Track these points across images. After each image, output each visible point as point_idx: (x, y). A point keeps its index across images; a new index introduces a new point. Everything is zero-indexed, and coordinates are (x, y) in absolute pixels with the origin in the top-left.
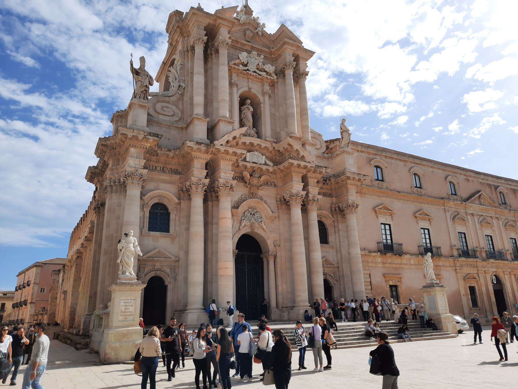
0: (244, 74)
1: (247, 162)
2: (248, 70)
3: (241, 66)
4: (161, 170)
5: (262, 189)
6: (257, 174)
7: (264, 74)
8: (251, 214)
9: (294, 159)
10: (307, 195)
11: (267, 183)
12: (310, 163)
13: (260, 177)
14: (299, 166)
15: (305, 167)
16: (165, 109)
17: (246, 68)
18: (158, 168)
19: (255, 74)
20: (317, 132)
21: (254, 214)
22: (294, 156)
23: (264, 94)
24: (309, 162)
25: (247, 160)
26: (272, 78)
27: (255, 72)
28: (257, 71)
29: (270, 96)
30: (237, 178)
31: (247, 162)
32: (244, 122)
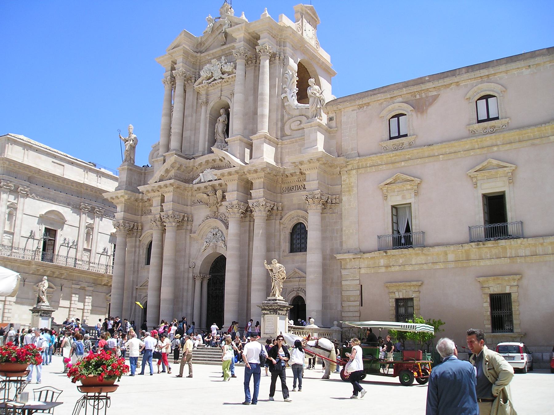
1: (203, 182)
17: (213, 79)
31: (203, 182)
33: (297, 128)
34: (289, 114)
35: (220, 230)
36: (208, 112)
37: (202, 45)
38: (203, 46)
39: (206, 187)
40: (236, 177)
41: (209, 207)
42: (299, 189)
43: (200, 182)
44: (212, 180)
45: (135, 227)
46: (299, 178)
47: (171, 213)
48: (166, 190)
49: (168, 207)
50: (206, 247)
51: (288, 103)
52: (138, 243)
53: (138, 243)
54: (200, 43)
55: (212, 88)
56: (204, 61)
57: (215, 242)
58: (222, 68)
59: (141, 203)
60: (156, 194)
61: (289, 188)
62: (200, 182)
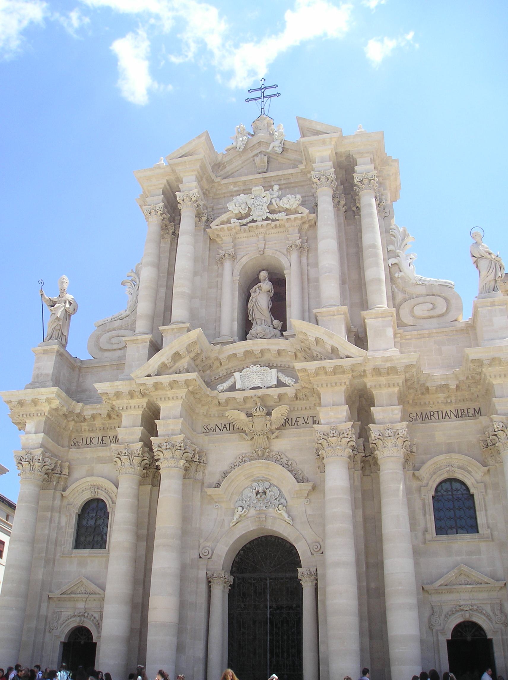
0: (245, 231)
1: (238, 390)
4: (99, 443)
5: (277, 437)
6: (258, 409)
8: (258, 493)
9: (321, 359)
11: (297, 421)
13: (269, 414)
16: (114, 340)
17: (250, 219)
18: (95, 441)
21: (265, 493)
22: (320, 353)
25: (238, 387)
27: (267, 219)
28: (270, 216)
30: (228, 426)
31: (238, 390)
33: (426, 314)
34: (404, 292)
35: (274, 485)
36: (237, 272)
37: (221, 168)
38: (221, 170)
39: (245, 399)
40: (346, 378)
41: (249, 438)
42: (447, 417)
43: (233, 388)
44: (260, 388)
45: (58, 469)
46: (448, 397)
47: (180, 441)
48: (169, 393)
49: (171, 427)
50: (240, 516)
51: (401, 274)
52: (58, 502)
53: (58, 502)
54: (219, 163)
55: (245, 235)
56: (224, 193)
57: (264, 508)
58: (271, 203)
59: (73, 422)
60: (133, 402)
61: (424, 415)
62: (233, 388)
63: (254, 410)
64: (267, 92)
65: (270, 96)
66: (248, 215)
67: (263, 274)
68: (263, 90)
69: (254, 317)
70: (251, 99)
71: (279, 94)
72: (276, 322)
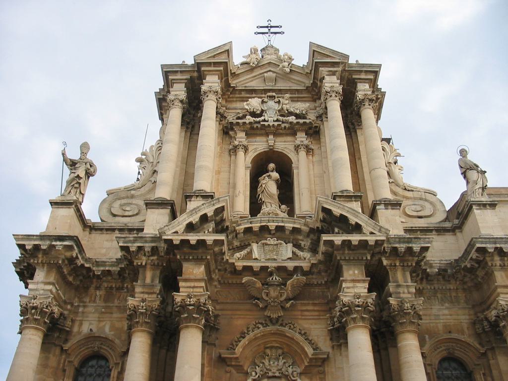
2: (264, 121)
3: (248, 117)
6: (274, 278)
7: (292, 119)
10: (382, 302)
12: (375, 234)
14: (347, 244)
15: (364, 244)
17: (263, 118)
19: (276, 124)
20: (422, 189)
23: (297, 148)
24: (372, 233)
26: (308, 121)
27: (277, 120)
28: (281, 118)
29: (309, 150)
32: (261, 199)
63: (271, 279)
64: (273, 30)
65: (275, 33)
66: (260, 115)
67: (272, 166)
68: (269, 28)
69: (263, 200)
70: (259, 33)
71: (284, 33)
72: (283, 207)
